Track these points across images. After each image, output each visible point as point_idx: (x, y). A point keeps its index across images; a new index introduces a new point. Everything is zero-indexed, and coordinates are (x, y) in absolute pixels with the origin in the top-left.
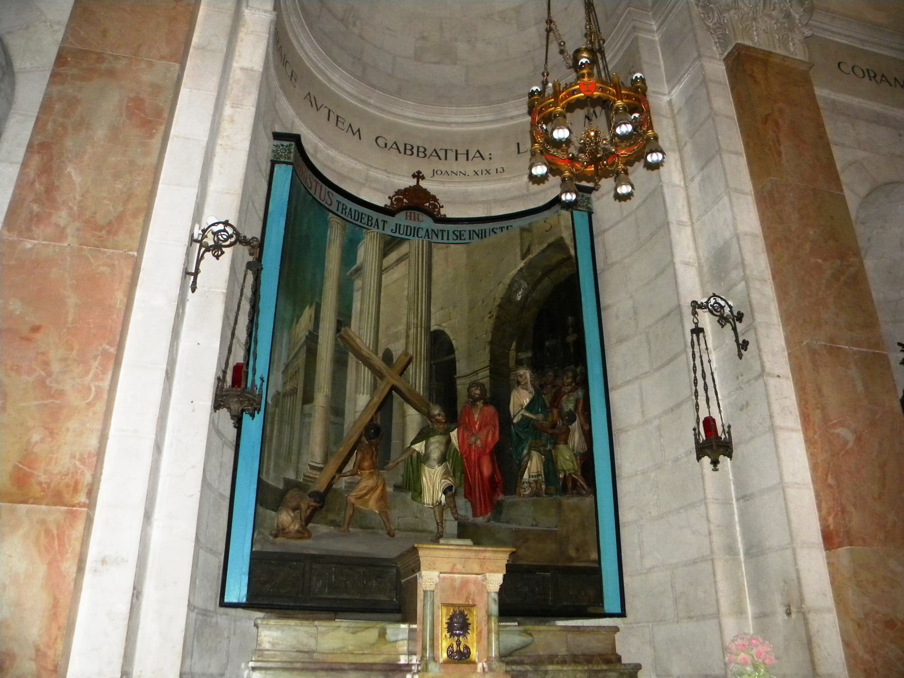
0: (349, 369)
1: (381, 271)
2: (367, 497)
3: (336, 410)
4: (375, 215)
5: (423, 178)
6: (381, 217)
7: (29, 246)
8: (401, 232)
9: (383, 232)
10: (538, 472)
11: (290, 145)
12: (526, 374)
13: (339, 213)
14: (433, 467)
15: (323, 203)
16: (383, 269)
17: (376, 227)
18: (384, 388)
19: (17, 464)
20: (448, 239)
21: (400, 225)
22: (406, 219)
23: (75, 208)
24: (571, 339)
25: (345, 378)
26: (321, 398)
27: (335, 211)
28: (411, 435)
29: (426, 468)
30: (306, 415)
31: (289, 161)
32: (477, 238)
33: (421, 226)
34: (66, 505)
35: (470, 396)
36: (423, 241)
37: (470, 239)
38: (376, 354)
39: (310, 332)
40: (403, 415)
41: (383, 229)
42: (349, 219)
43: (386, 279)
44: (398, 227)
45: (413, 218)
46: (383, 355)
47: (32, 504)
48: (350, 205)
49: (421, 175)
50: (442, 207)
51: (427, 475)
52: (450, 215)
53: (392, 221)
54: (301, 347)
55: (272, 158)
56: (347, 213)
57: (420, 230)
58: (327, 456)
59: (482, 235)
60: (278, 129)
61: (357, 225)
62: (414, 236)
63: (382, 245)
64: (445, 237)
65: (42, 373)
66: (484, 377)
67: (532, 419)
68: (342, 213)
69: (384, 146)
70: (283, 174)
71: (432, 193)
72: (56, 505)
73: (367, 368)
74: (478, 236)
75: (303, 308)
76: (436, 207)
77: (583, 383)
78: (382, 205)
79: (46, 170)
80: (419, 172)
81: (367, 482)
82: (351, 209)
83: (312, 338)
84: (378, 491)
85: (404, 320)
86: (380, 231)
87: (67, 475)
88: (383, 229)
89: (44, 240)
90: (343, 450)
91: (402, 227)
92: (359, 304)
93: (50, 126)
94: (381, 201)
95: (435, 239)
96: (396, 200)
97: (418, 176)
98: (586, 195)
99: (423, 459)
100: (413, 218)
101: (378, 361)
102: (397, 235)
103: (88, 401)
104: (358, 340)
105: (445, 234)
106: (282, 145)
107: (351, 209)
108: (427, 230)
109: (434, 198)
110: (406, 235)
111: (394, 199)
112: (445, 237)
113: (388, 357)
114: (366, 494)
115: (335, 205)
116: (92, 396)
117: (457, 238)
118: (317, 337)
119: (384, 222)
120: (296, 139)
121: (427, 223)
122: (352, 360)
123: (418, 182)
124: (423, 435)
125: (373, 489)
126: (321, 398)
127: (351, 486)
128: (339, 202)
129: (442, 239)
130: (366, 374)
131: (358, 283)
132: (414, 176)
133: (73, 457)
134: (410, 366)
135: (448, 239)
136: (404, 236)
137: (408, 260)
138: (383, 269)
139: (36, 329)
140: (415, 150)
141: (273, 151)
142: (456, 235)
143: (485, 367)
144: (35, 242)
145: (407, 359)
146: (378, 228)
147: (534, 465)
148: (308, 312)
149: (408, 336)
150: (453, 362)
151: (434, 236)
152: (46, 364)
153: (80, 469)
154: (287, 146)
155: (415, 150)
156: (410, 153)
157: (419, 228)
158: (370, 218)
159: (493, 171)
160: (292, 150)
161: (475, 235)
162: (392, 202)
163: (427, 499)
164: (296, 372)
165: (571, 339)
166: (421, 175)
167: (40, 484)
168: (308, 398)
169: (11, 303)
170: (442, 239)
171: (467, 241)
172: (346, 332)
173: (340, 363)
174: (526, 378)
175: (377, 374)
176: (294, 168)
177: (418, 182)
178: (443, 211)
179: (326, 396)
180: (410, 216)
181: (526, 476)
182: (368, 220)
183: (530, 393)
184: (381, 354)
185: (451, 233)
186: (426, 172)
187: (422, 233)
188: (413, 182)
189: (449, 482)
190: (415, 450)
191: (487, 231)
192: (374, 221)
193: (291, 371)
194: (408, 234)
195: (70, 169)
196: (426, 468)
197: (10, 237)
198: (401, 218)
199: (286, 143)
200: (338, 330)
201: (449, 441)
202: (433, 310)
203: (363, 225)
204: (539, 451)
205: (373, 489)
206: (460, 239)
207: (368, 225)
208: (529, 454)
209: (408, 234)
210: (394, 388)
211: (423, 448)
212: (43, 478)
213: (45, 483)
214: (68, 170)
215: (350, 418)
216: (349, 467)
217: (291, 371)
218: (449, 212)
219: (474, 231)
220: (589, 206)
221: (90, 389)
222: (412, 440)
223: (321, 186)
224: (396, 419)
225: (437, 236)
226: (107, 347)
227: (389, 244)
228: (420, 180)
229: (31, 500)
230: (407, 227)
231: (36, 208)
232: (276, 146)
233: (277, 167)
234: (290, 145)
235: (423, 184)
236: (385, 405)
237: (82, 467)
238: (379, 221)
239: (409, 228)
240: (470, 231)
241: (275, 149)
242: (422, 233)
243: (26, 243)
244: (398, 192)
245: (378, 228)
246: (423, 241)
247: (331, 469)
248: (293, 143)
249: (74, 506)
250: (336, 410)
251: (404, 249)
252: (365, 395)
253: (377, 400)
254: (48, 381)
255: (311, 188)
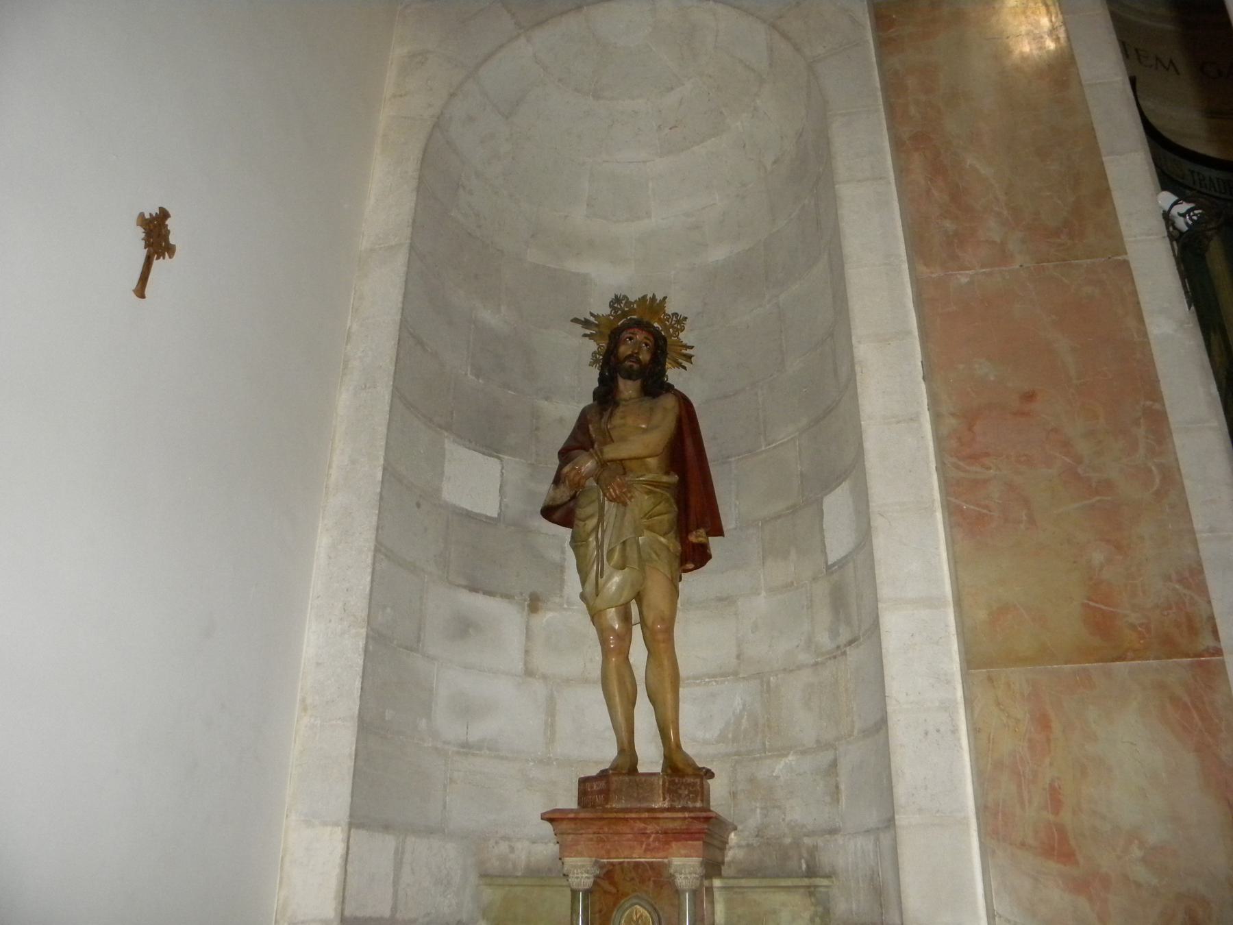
7: (964, 280)
19: (1086, 601)
23: (1005, 212)
34: (1187, 656)
47: (1133, 659)
65: (1067, 460)
72: (1171, 658)
79: (937, 170)
87: (1171, 608)
89: (982, 267)
93: (913, 110)
103: (1155, 488)
116: (1157, 481)
133: (1169, 578)
139: (1029, 397)
144: (970, 272)
152: (1066, 445)
153: (1185, 594)
167: (1133, 627)
169: (977, 366)
195: (970, 160)
197: (932, 273)
212: (1134, 618)
213: (1141, 625)
214: (968, 163)
221: (1150, 471)
226: (1149, 403)
229: (1130, 654)
231: (948, 225)
237: (1185, 591)
243: (959, 276)
249: (1201, 655)
254: (1080, 470)
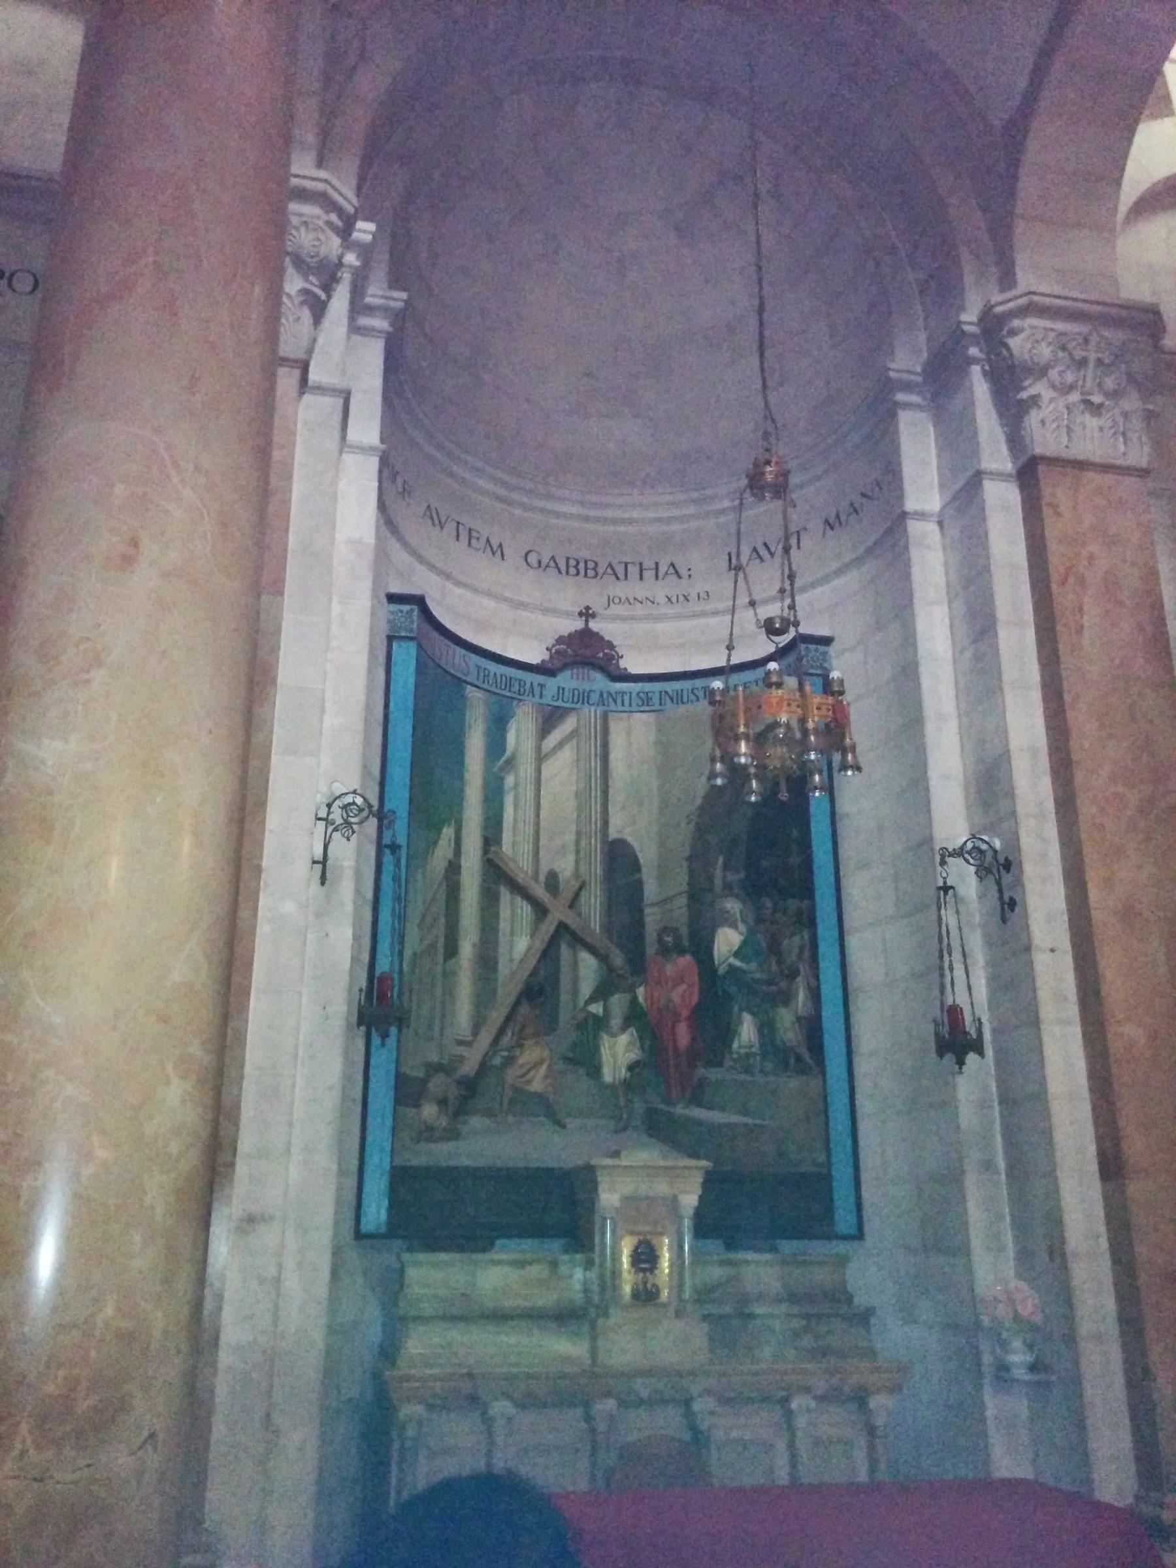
0: (502, 904)
1: (540, 758)
2: (532, 1073)
3: (487, 961)
4: (528, 677)
5: (593, 616)
6: (539, 679)
8: (565, 700)
9: (541, 701)
10: (750, 1041)
11: (412, 611)
12: (733, 906)
13: (479, 684)
14: (614, 1035)
15: (460, 675)
16: (542, 755)
17: (531, 695)
18: (549, 926)
20: (630, 705)
21: (563, 689)
22: (572, 678)
24: (794, 860)
25: (497, 916)
26: (467, 948)
27: (476, 682)
28: (586, 990)
29: (605, 1037)
30: (449, 975)
31: (412, 635)
32: (671, 705)
33: (593, 688)
35: (660, 941)
36: (595, 711)
37: (661, 704)
38: (537, 881)
39: (450, 862)
40: (575, 966)
41: (541, 697)
42: (493, 689)
43: (547, 769)
44: (561, 690)
45: (581, 677)
46: (547, 878)
48: (493, 667)
49: (591, 612)
50: (622, 657)
51: (607, 1045)
52: (634, 669)
53: (552, 684)
54: (440, 884)
55: (389, 633)
56: (491, 682)
57: (592, 694)
58: (478, 1024)
59: (678, 699)
60: (396, 588)
61: (503, 696)
62: (583, 703)
63: (540, 721)
64: (627, 703)
66: (680, 908)
67: (739, 969)
68: (484, 682)
69: (535, 564)
70: (406, 655)
71: (607, 638)
73: (525, 902)
74: (672, 699)
75: (439, 831)
76: (611, 658)
77: (810, 922)
78: (534, 662)
80: (588, 608)
81: (530, 1054)
82: (495, 674)
83: (454, 868)
84: (544, 1067)
85: (573, 828)
86: (537, 699)
88: (541, 697)
90: (497, 1016)
91: (566, 693)
92: (512, 813)
94: (534, 654)
95: (612, 706)
96: (557, 652)
97: (587, 614)
98: (822, 648)
99: (600, 1024)
100: (581, 677)
101: (540, 892)
102: (560, 703)
104: (512, 865)
105: (626, 698)
106: (402, 612)
107: (495, 674)
108: (601, 695)
109: (611, 646)
110: (573, 702)
111: (553, 651)
112: (627, 703)
113: (552, 884)
114: (529, 1071)
115: (474, 671)
117: (643, 704)
118: (460, 867)
119: (542, 686)
120: (419, 601)
121: (599, 682)
122: (505, 895)
123: (587, 621)
124: (602, 993)
125: (537, 1064)
126: (467, 948)
127: (509, 1061)
128: (478, 667)
129: (623, 705)
130: (525, 910)
131: (510, 780)
132: (581, 614)
134: (583, 893)
135: (630, 705)
136: (568, 705)
137: (574, 741)
138: (542, 755)
140: (581, 566)
141: (389, 621)
142: (641, 698)
143: (681, 893)
145: (577, 885)
146: (534, 696)
147: (747, 1031)
148: (448, 832)
149: (578, 852)
150: (639, 885)
151: (611, 700)
154: (407, 613)
155: (582, 566)
156: (575, 572)
157: (590, 691)
158: (522, 683)
159: (694, 596)
160: (415, 618)
161: (667, 698)
162: (551, 657)
163: (608, 1076)
164: (435, 920)
165: (794, 860)
166: (591, 612)
168: (452, 951)
170: (623, 705)
171: (657, 707)
172: (496, 853)
173: (489, 899)
174: (735, 913)
175: (541, 910)
176: (420, 646)
177: (587, 621)
178: (623, 664)
179: (474, 946)
180: (578, 675)
181: (735, 1045)
182: (520, 686)
183: (741, 934)
184: (542, 878)
185: (634, 695)
186: (597, 606)
187: (595, 697)
188: (579, 624)
189: (634, 1055)
190: (589, 1012)
191: (685, 693)
192: (528, 686)
193: (429, 919)
194: (576, 700)
196: (605, 1037)
198: (566, 680)
199: (406, 608)
200: (486, 852)
201: (635, 998)
202: (611, 810)
203: (514, 695)
204: (753, 1014)
205: (537, 1064)
206: (648, 705)
207: (519, 694)
208: (739, 1017)
209: (576, 700)
210: (562, 927)
211: (601, 1010)
215: (503, 970)
216: (506, 1040)
217: (429, 919)
218: (633, 664)
219: (666, 692)
220: (826, 665)
222: (587, 997)
223: (454, 650)
224: (565, 968)
225: (615, 701)
227: (549, 719)
228: (590, 619)
230: (574, 690)
232: (393, 613)
233: (395, 645)
234: (412, 611)
235: (594, 625)
236: (549, 953)
238: (535, 684)
239: (576, 692)
240: (661, 692)
241: (392, 617)
242: (595, 697)
244: (560, 640)
245: (534, 696)
246: (595, 711)
247: (485, 1038)
248: (415, 607)
250: (487, 961)
251: (569, 724)
252: (524, 937)
253: (540, 945)
255: (440, 659)
